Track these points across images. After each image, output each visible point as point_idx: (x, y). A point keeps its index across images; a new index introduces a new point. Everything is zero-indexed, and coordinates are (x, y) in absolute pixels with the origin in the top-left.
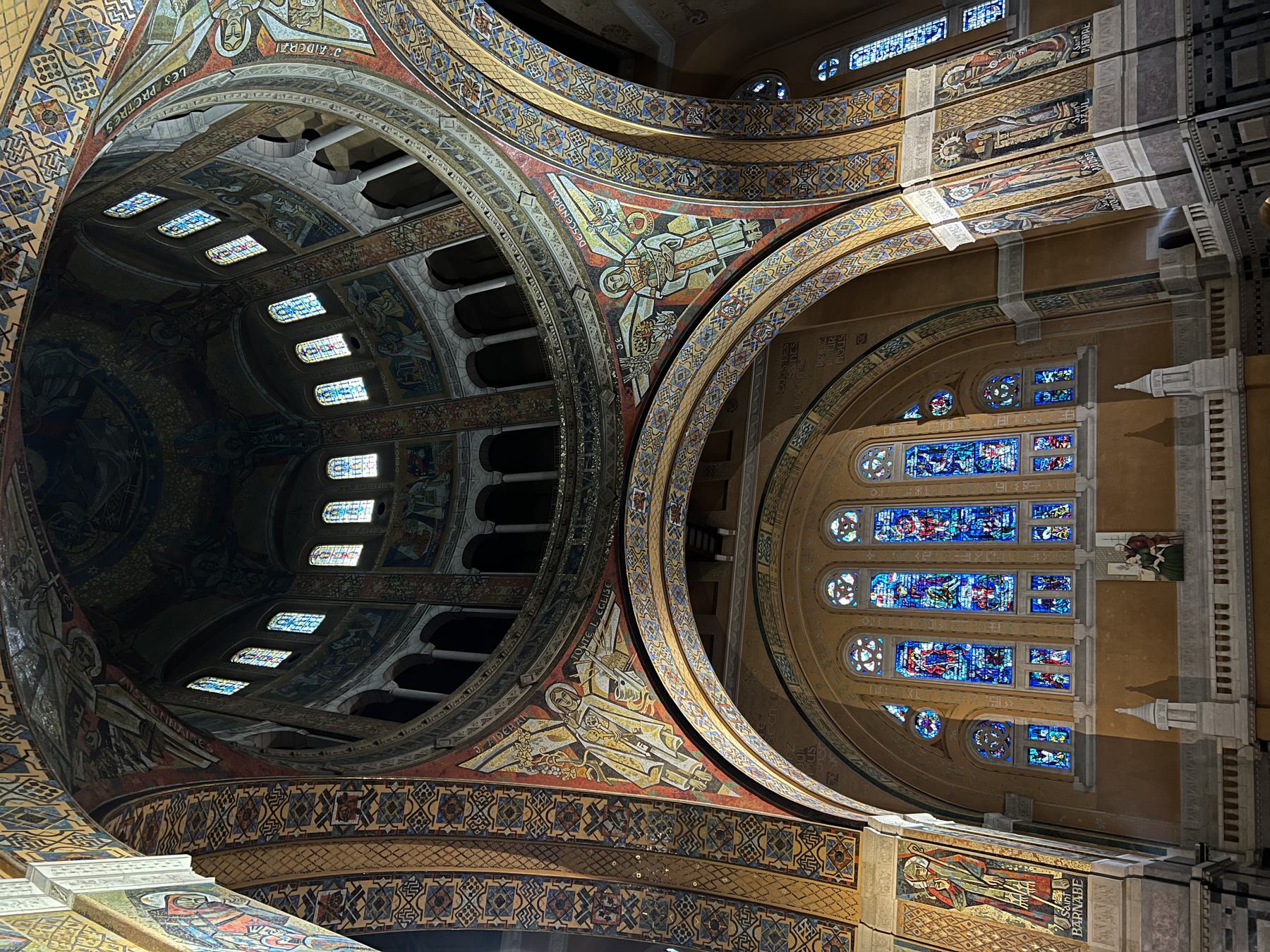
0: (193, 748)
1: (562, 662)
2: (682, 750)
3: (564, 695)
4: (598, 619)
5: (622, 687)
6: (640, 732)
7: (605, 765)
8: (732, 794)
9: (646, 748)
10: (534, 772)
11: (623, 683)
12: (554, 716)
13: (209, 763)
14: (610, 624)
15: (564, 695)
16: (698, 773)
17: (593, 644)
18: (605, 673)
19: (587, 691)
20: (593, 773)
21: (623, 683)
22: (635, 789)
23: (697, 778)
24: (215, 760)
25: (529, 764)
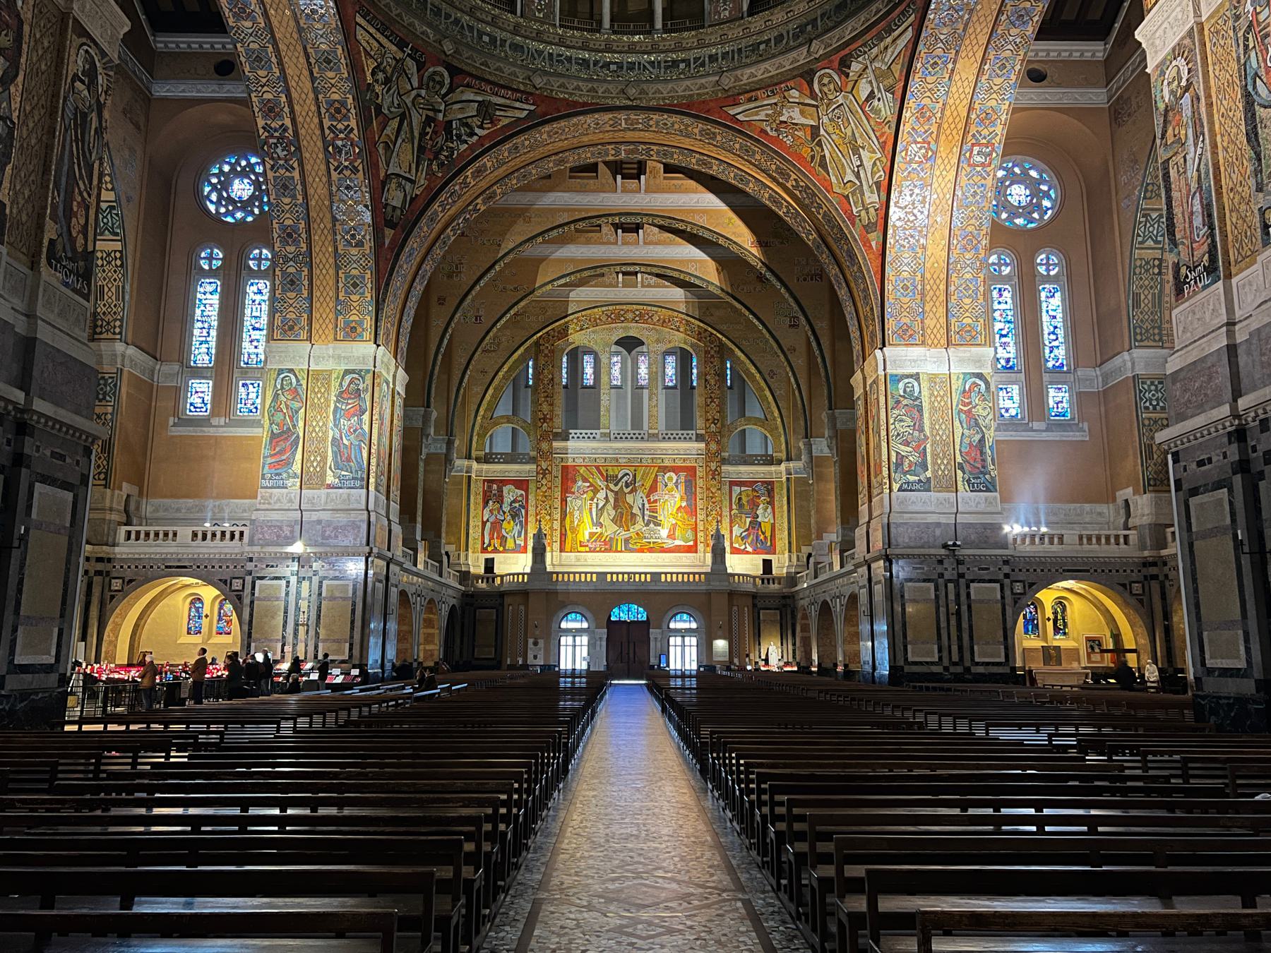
0: (517, 105)
1: (843, 53)
2: (878, 184)
3: (830, 82)
4: (891, 31)
5: (876, 102)
6: (863, 148)
7: (824, 156)
8: (873, 244)
9: (859, 163)
10: (774, 134)
11: (879, 100)
12: (813, 95)
13: (527, 112)
14: (898, 42)
15: (830, 82)
16: (872, 211)
17: (875, 51)
18: (870, 82)
19: (849, 89)
20: (813, 157)
21: (879, 100)
22: (829, 188)
23: (867, 213)
24: (532, 108)
25: (774, 126)
